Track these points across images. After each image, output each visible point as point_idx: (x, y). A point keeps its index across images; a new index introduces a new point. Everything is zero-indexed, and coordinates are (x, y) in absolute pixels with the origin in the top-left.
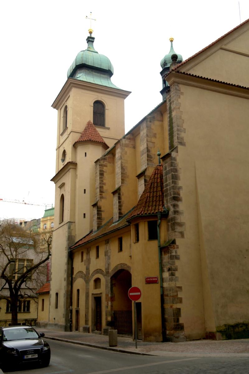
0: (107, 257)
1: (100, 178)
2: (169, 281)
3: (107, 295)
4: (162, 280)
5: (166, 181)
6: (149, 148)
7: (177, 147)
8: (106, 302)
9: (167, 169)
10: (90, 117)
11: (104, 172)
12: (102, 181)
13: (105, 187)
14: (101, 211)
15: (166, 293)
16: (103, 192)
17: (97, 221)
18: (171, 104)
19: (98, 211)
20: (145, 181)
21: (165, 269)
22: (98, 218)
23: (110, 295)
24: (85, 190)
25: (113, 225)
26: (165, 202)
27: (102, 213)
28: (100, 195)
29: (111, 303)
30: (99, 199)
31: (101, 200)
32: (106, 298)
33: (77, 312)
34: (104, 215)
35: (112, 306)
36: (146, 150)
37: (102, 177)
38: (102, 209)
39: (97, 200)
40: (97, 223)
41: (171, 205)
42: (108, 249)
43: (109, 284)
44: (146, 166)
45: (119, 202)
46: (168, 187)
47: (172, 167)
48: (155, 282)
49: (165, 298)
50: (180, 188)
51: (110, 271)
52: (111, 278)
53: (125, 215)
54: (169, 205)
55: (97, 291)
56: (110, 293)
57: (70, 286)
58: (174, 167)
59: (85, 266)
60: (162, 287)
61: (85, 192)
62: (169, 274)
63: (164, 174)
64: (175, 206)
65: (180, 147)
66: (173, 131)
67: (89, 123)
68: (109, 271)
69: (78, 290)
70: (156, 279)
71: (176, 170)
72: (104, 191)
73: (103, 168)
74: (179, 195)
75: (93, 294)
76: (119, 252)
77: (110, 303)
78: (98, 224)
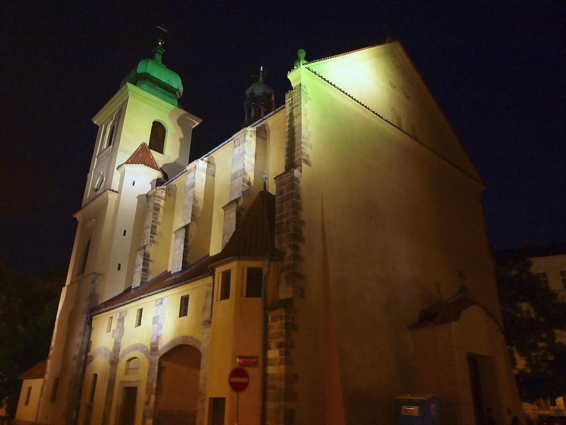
0: (156, 325)
1: (154, 213)
2: (280, 364)
3: (149, 384)
4: (266, 362)
5: (282, 211)
6: (246, 171)
7: (300, 165)
8: (147, 396)
9: (285, 194)
10: (146, 139)
11: (160, 206)
12: (157, 219)
13: (159, 228)
14: (149, 260)
15: (270, 383)
16: (156, 234)
17: (142, 274)
18: (292, 109)
19: (144, 259)
20: (238, 214)
21: (273, 344)
22: (144, 270)
23: (155, 385)
24: (125, 232)
25: (170, 278)
26: (276, 241)
27: (150, 264)
28: (151, 237)
29: (156, 398)
30: (149, 242)
31: (151, 245)
32: (147, 389)
33: (90, 408)
34: (151, 266)
35: (156, 403)
36: (242, 172)
37: (157, 214)
38: (151, 258)
39: (145, 244)
40: (140, 276)
41: (289, 246)
42: (159, 313)
43: (157, 368)
44: (239, 194)
45: (185, 246)
46: (284, 220)
47: (294, 191)
48: (254, 364)
49: (269, 391)
50: (303, 223)
51: (160, 347)
52: (160, 358)
53: (191, 266)
54: (285, 245)
55: (131, 378)
56: (156, 381)
57: (82, 369)
58: (297, 191)
59: (114, 339)
60: (265, 375)
61: (124, 235)
62: (280, 353)
63: (277, 201)
64: (296, 248)
65: (304, 165)
66: (295, 144)
67: (143, 145)
68: (157, 348)
69: (96, 375)
70: (255, 360)
71: (298, 197)
72: (157, 233)
73: (160, 201)
74: (302, 233)
75: (122, 382)
76: (180, 316)
77: (153, 397)
78: (142, 278)
